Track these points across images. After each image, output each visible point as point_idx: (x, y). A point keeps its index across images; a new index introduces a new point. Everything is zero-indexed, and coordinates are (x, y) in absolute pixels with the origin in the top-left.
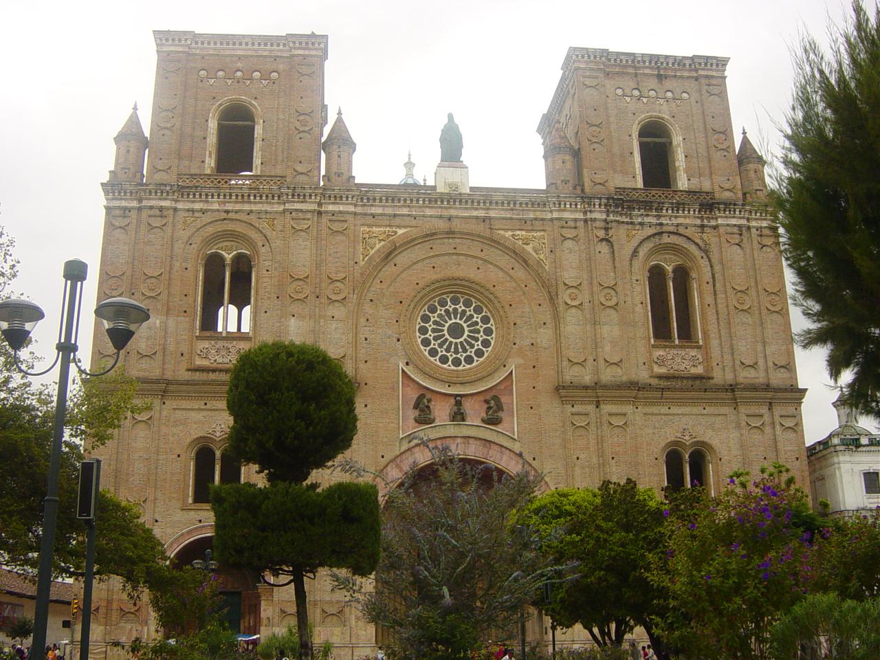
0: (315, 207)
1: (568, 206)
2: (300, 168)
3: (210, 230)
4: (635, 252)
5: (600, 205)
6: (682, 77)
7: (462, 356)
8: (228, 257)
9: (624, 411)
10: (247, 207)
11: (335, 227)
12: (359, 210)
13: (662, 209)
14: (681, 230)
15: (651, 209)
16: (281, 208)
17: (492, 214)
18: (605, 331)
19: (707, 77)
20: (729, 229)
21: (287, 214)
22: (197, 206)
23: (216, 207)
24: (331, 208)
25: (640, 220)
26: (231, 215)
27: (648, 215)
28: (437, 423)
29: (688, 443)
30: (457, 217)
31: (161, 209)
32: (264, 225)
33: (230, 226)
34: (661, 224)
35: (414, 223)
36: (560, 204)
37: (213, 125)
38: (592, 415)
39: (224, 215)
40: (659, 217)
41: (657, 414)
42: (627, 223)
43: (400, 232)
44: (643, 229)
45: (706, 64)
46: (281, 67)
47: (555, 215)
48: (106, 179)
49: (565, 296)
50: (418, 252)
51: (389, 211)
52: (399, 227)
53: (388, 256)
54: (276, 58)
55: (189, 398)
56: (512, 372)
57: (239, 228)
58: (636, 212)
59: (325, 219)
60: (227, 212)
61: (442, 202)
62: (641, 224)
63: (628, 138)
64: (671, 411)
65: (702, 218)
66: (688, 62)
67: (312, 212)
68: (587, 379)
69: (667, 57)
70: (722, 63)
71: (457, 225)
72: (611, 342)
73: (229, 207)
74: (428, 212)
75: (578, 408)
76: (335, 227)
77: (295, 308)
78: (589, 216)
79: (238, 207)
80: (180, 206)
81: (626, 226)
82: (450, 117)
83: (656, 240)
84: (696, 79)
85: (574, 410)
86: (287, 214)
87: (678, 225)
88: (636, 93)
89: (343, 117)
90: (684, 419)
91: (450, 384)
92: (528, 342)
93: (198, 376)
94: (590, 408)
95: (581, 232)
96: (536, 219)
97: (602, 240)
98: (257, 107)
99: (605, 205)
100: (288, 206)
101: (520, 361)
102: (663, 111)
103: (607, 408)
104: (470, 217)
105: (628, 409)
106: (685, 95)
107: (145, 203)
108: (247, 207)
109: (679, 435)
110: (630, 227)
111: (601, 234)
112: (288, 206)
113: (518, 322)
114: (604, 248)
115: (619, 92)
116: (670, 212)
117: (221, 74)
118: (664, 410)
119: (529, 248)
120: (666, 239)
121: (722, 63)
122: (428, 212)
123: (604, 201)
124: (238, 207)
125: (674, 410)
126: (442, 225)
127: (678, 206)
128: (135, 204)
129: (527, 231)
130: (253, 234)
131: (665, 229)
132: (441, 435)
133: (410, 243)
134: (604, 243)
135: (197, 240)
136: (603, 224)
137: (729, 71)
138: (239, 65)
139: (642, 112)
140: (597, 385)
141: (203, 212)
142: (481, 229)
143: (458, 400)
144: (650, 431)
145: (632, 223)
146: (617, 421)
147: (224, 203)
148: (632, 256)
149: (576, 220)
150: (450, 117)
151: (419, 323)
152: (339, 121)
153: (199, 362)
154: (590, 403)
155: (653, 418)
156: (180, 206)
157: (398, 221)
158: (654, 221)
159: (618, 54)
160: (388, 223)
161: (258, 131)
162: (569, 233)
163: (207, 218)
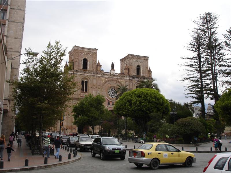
0: (96, 75)
2: (94, 69)
3: (83, 77)
7: (111, 96)
8: (85, 81)
11: (99, 78)
16: (92, 75)
17: (118, 78)
22: (81, 74)
23: (83, 74)
24: (98, 75)
31: (76, 74)
32: (89, 77)
33: (85, 77)
37: (82, 61)
46: (91, 53)
47: (126, 78)
50: (109, 82)
51: (105, 76)
53: (105, 82)
54: (91, 52)
57: (87, 77)
59: (97, 77)
70: (148, 57)
71: (114, 79)
73: (85, 74)
74: (110, 77)
76: (99, 78)
77: (94, 89)
79: (86, 74)
82: (113, 62)
83: (137, 82)
84: (145, 59)
89: (99, 61)
91: (112, 100)
93: (81, 98)
95: (129, 81)
98: (88, 59)
100: (93, 75)
102: (140, 64)
107: (74, 73)
111: (131, 81)
112: (93, 75)
114: (131, 83)
117: (83, 53)
121: (148, 57)
122: (110, 77)
124: (86, 74)
126: (112, 79)
127: (141, 78)
128: (73, 73)
130: (89, 79)
133: (108, 81)
137: (149, 59)
138: (86, 52)
142: (117, 80)
143: (113, 102)
151: (108, 92)
152: (99, 62)
153: (81, 96)
156: (79, 73)
157: (106, 78)
161: (88, 63)
162: (127, 81)
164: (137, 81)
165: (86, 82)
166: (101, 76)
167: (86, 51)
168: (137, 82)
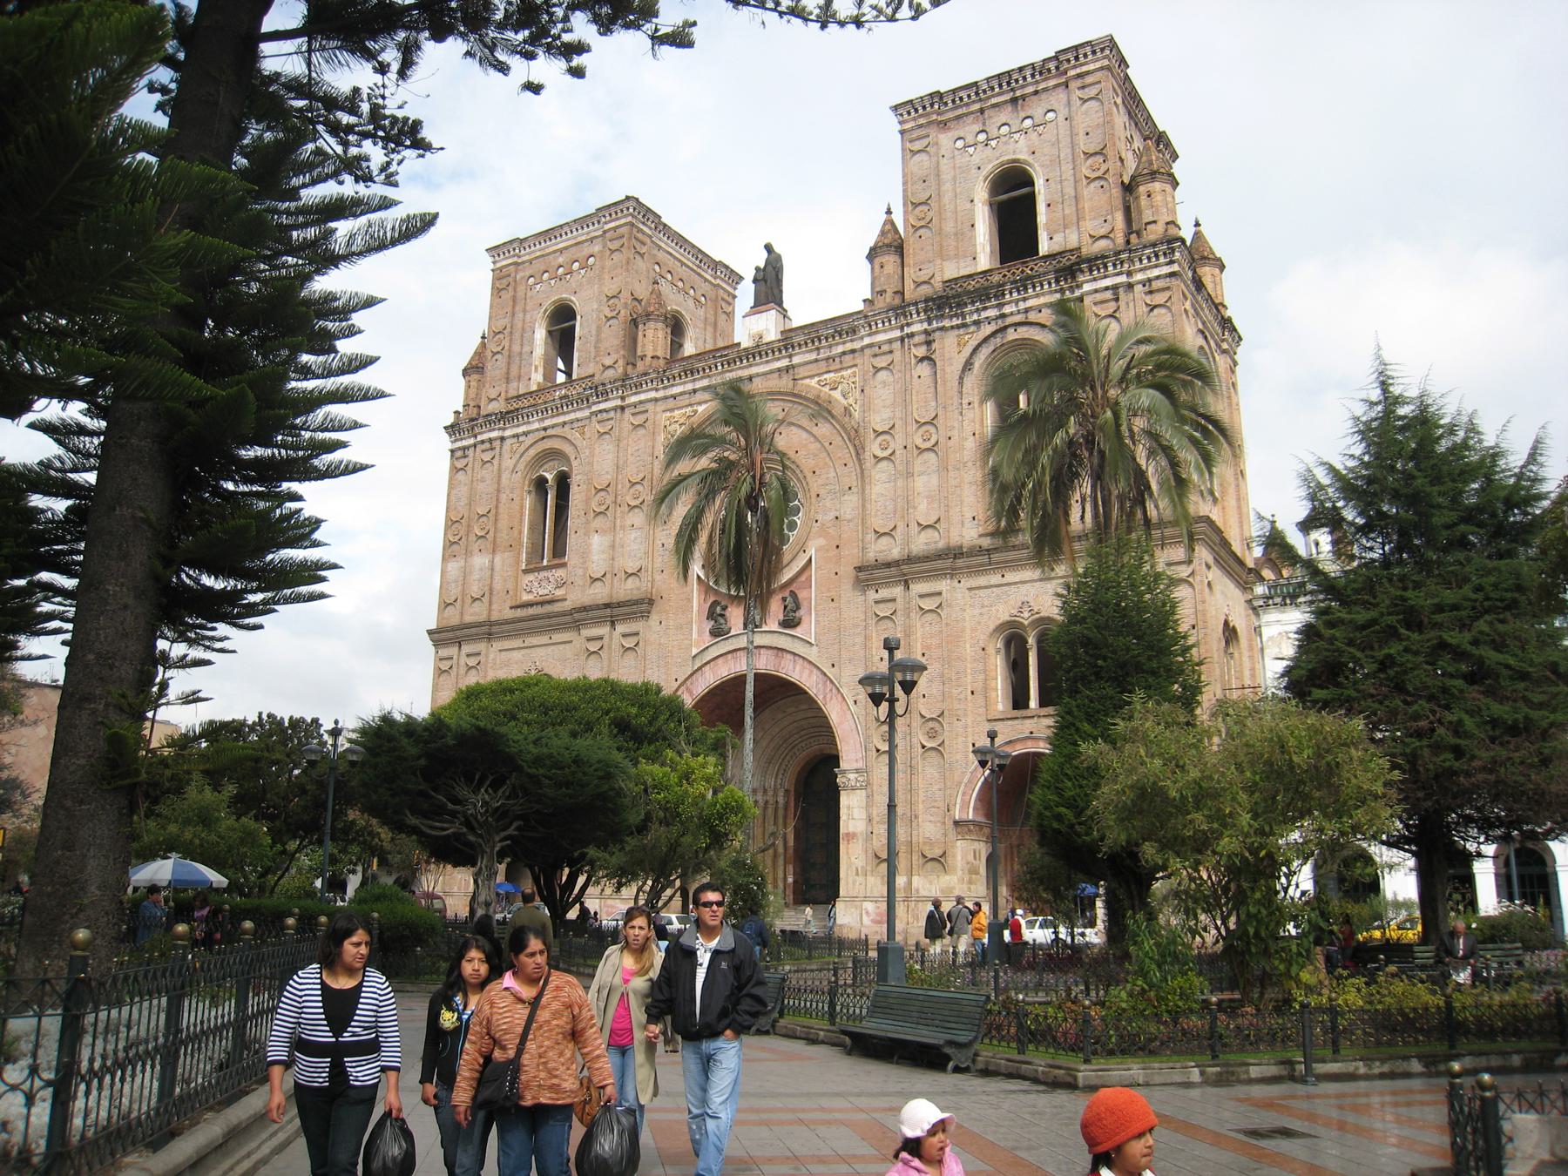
0: (619, 402)
1: (880, 325)
3: (532, 452)
4: (968, 366)
6: (1045, 90)
9: (938, 589)
10: (561, 419)
12: (661, 394)
13: (1004, 295)
14: (1032, 317)
15: (989, 299)
18: (920, 483)
19: (1080, 76)
20: (1099, 297)
21: (593, 418)
22: (523, 429)
24: (634, 399)
25: (975, 317)
26: (550, 432)
27: (985, 309)
28: (732, 633)
29: (1026, 623)
30: (758, 375)
31: (490, 440)
33: (548, 444)
34: (1003, 316)
36: (870, 326)
38: (900, 604)
39: (543, 434)
40: (1000, 306)
41: (986, 587)
42: (958, 327)
43: (701, 409)
44: (979, 329)
45: (1077, 58)
47: (867, 341)
48: (450, 420)
49: (874, 448)
51: (689, 387)
52: (700, 403)
55: (508, 637)
56: (810, 559)
58: (969, 308)
60: (545, 429)
61: (741, 361)
62: (977, 323)
63: (968, 205)
64: (1005, 581)
65: (1062, 291)
66: (1052, 66)
67: (615, 409)
68: (896, 553)
69: (1021, 69)
72: (928, 497)
73: (547, 423)
75: (884, 593)
78: (907, 330)
80: (508, 433)
81: (956, 332)
83: (998, 340)
85: (878, 596)
86: (593, 418)
87: (1027, 311)
88: (982, 137)
90: (1024, 588)
92: (832, 515)
93: (519, 613)
94: (897, 591)
95: (897, 355)
96: (844, 353)
97: (922, 360)
99: (925, 311)
100: (595, 408)
101: (821, 542)
102: (1018, 149)
103: (918, 588)
104: (771, 372)
105: (943, 585)
106: (1051, 115)
107: (480, 438)
108: (561, 419)
109: (1014, 612)
110: (962, 331)
113: (822, 492)
114: (924, 370)
115: (960, 144)
116: (1015, 294)
118: (995, 579)
119: (837, 394)
120: (1011, 335)
123: (921, 305)
125: (1011, 577)
129: (836, 371)
131: (1009, 320)
132: (733, 648)
134: (925, 363)
135: (521, 466)
136: (922, 338)
138: (561, 260)
139: (990, 161)
140: (910, 560)
141: (525, 434)
142: (784, 383)
144: (977, 611)
145: (964, 325)
146: (928, 604)
147: (543, 420)
148: (963, 371)
149: (890, 342)
150: (768, 248)
154: (897, 583)
155: (982, 593)
158: (992, 313)
159: (954, 91)
160: (687, 402)
162: (881, 362)
163: (529, 440)
164: (987, 329)
165: (563, 482)
166: (653, 394)
167: (561, 251)
168: (986, 340)
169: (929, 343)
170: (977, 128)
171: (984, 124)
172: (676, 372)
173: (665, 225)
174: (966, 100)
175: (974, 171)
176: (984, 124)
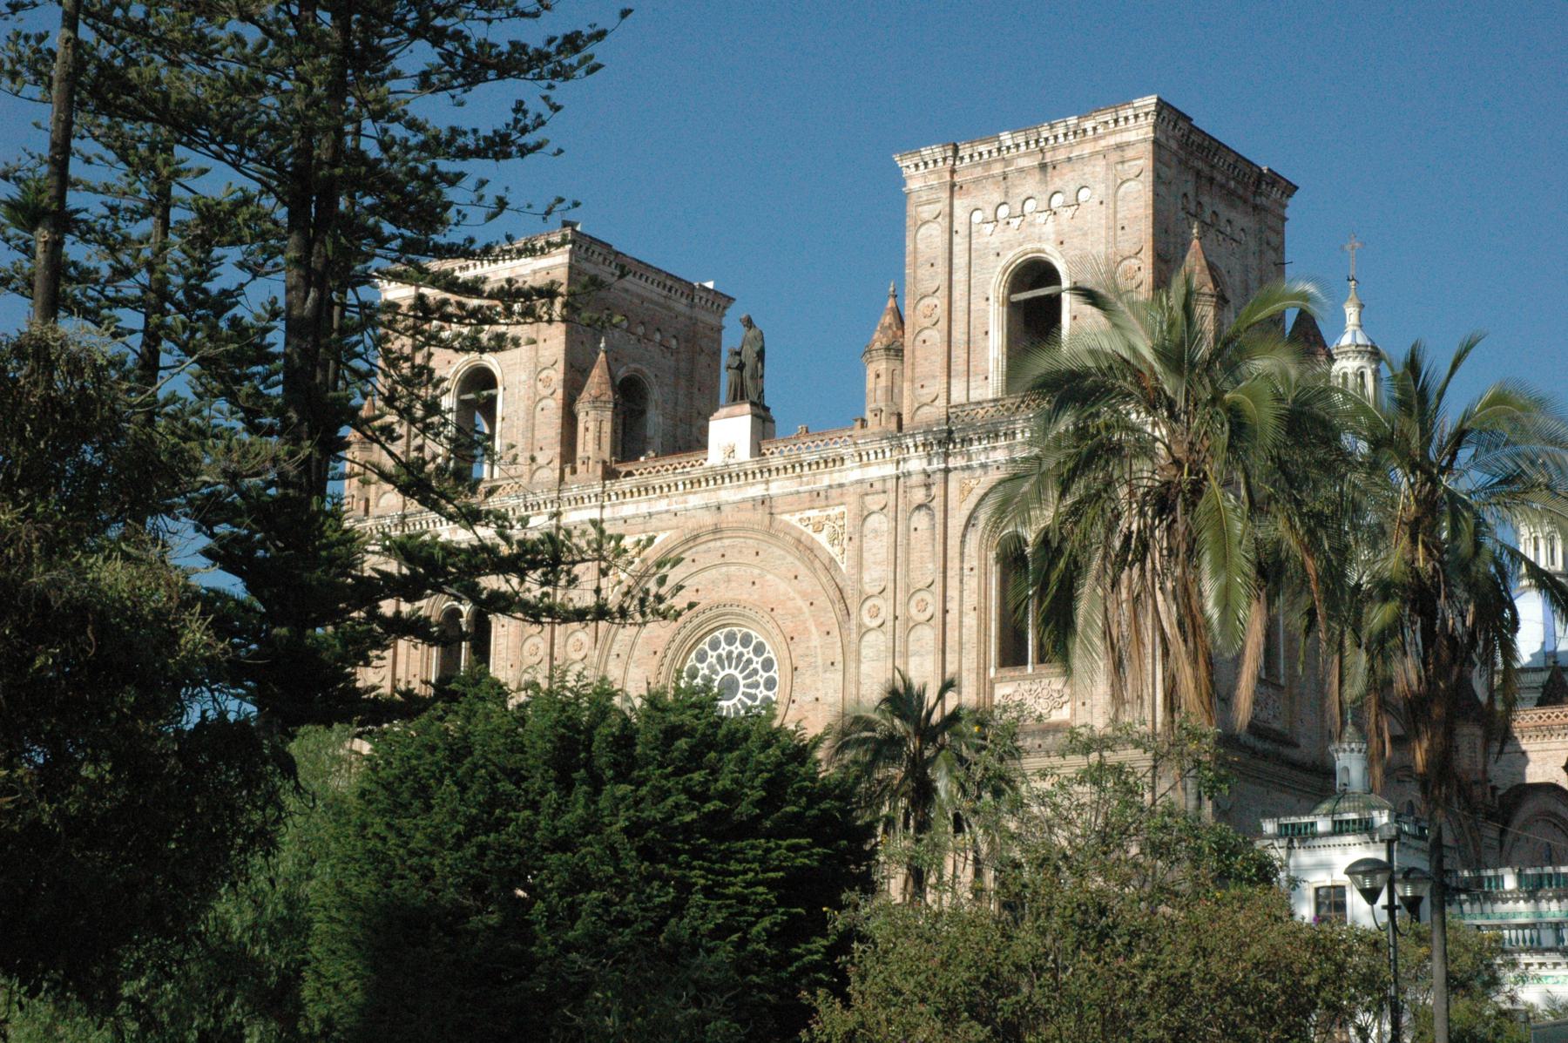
4: (970, 521)
5: (916, 446)
6: (1080, 157)
13: (1014, 433)
25: (983, 459)
35: (674, 521)
42: (963, 469)
45: (1116, 121)
58: (975, 447)
62: (984, 466)
92: (810, 697)
97: (919, 507)
110: (966, 474)
113: (800, 664)
119: (822, 539)
123: (920, 439)
126: (708, 519)
134: (923, 512)
139: (1011, 247)
145: (969, 468)
148: (966, 527)
149: (884, 479)
169: (928, 486)
170: (997, 197)
171: (1006, 194)
172: (627, 488)
173: (617, 253)
174: (986, 156)
175: (992, 257)
176: (1006, 194)
